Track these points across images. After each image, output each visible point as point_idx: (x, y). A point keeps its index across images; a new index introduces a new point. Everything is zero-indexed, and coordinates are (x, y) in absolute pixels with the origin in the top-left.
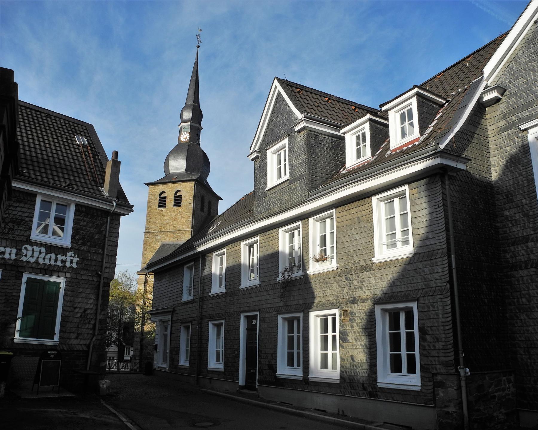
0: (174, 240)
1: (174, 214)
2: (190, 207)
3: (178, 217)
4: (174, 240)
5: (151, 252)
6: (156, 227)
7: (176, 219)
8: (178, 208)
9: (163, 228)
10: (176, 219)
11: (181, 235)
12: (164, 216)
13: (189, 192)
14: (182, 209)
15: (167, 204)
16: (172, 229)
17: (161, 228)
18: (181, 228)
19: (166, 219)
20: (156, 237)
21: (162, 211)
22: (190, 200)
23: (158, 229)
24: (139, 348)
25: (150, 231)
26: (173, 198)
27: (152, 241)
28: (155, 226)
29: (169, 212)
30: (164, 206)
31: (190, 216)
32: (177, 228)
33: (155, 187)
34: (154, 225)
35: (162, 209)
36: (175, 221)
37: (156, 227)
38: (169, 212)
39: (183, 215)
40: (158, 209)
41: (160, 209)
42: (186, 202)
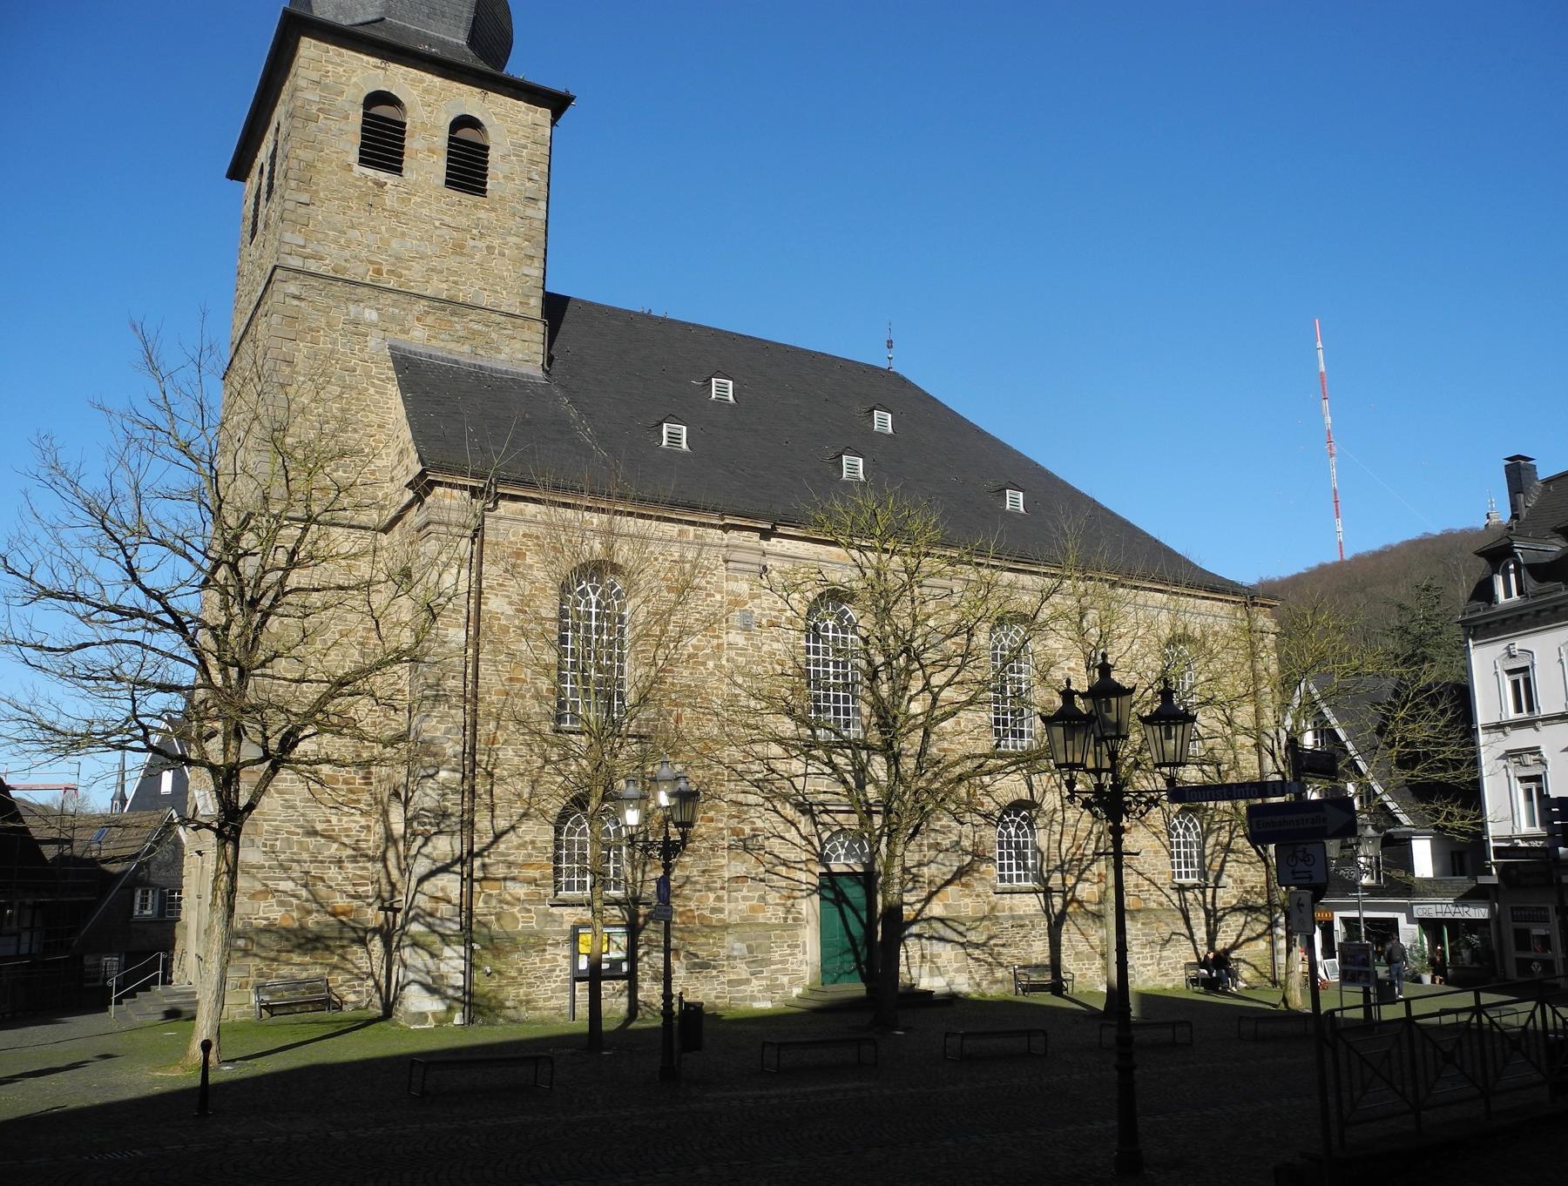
0: (452, 345)
1: (448, 220)
2: (529, 212)
3: (472, 243)
4: (452, 345)
6: (347, 253)
7: (459, 249)
8: (468, 199)
9: (389, 272)
10: (459, 249)
11: (494, 336)
12: (395, 214)
13: (525, 147)
14: (494, 210)
16: (437, 287)
17: (378, 272)
18: (485, 300)
19: (403, 234)
20: (352, 307)
21: (381, 185)
23: (358, 271)
25: (312, 266)
26: (441, 141)
27: (329, 325)
28: (342, 248)
29: (420, 205)
30: (394, 165)
31: (531, 258)
32: (464, 294)
33: (340, 55)
34: (336, 242)
35: (382, 176)
36: (458, 259)
37: (347, 253)
38: (420, 205)
39: (496, 242)
41: (370, 172)
42: (510, 185)
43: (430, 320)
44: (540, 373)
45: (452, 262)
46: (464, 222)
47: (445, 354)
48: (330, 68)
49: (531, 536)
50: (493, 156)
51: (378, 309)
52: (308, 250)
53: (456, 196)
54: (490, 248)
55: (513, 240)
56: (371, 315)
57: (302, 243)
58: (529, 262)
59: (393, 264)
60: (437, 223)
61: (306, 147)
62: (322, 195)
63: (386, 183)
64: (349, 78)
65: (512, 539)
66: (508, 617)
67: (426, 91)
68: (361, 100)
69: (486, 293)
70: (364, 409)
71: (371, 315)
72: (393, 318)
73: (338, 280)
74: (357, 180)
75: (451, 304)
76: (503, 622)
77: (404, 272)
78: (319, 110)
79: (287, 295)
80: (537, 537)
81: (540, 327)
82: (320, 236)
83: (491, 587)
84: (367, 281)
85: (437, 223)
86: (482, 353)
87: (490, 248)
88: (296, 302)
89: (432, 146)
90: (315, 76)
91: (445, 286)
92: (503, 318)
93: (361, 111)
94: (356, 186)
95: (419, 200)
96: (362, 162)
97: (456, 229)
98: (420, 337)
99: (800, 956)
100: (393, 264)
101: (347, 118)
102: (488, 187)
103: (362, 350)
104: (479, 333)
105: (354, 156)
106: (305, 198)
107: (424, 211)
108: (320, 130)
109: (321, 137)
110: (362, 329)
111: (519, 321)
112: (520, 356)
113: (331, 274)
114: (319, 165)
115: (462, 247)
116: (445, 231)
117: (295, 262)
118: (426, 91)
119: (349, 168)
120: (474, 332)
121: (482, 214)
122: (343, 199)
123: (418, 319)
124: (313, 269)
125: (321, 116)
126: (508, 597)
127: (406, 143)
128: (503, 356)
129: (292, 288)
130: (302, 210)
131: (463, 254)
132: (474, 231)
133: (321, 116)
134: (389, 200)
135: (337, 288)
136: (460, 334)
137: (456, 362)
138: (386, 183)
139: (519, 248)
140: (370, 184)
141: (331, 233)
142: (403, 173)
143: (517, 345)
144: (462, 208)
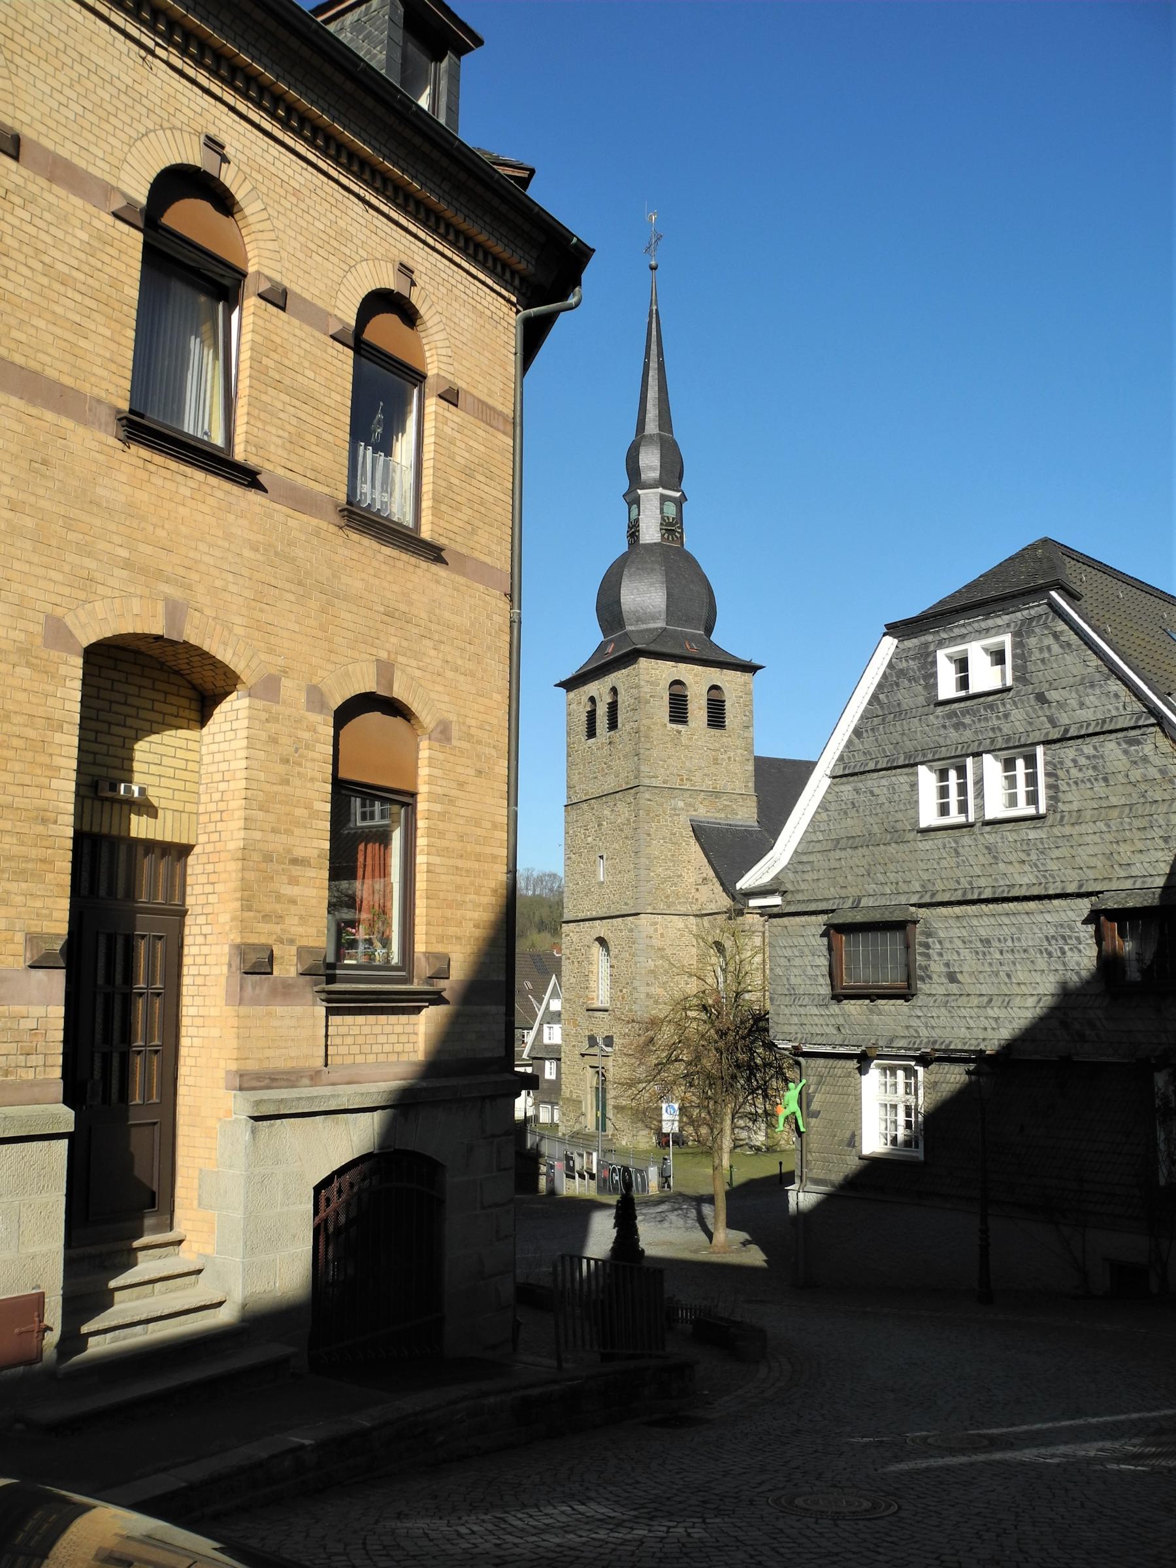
4: (717, 815)
5: (662, 841)
6: (668, 772)
7: (716, 761)
8: (717, 732)
11: (734, 806)
12: (687, 747)
14: (730, 736)
16: (708, 784)
17: (682, 780)
19: (691, 757)
21: (679, 732)
22: (744, 718)
23: (675, 782)
27: (664, 812)
28: (666, 770)
31: (748, 760)
34: (663, 767)
35: (680, 727)
39: (732, 754)
41: (674, 726)
43: (706, 803)
44: (756, 824)
45: (713, 769)
47: (713, 820)
48: (653, 672)
50: (728, 705)
53: (713, 732)
54: (729, 758)
55: (739, 751)
56: (681, 804)
67: (696, 675)
71: (681, 804)
72: (690, 805)
75: (716, 794)
81: (755, 799)
90: (647, 678)
98: (704, 812)
102: (726, 723)
104: (728, 806)
105: (667, 718)
109: (652, 710)
115: (717, 759)
117: (646, 781)
118: (696, 675)
121: (724, 739)
128: (739, 817)
129: (647, 796)
130: (647, 753)
134: (684, 741)
137: (720, 824)
139: (742, 755)
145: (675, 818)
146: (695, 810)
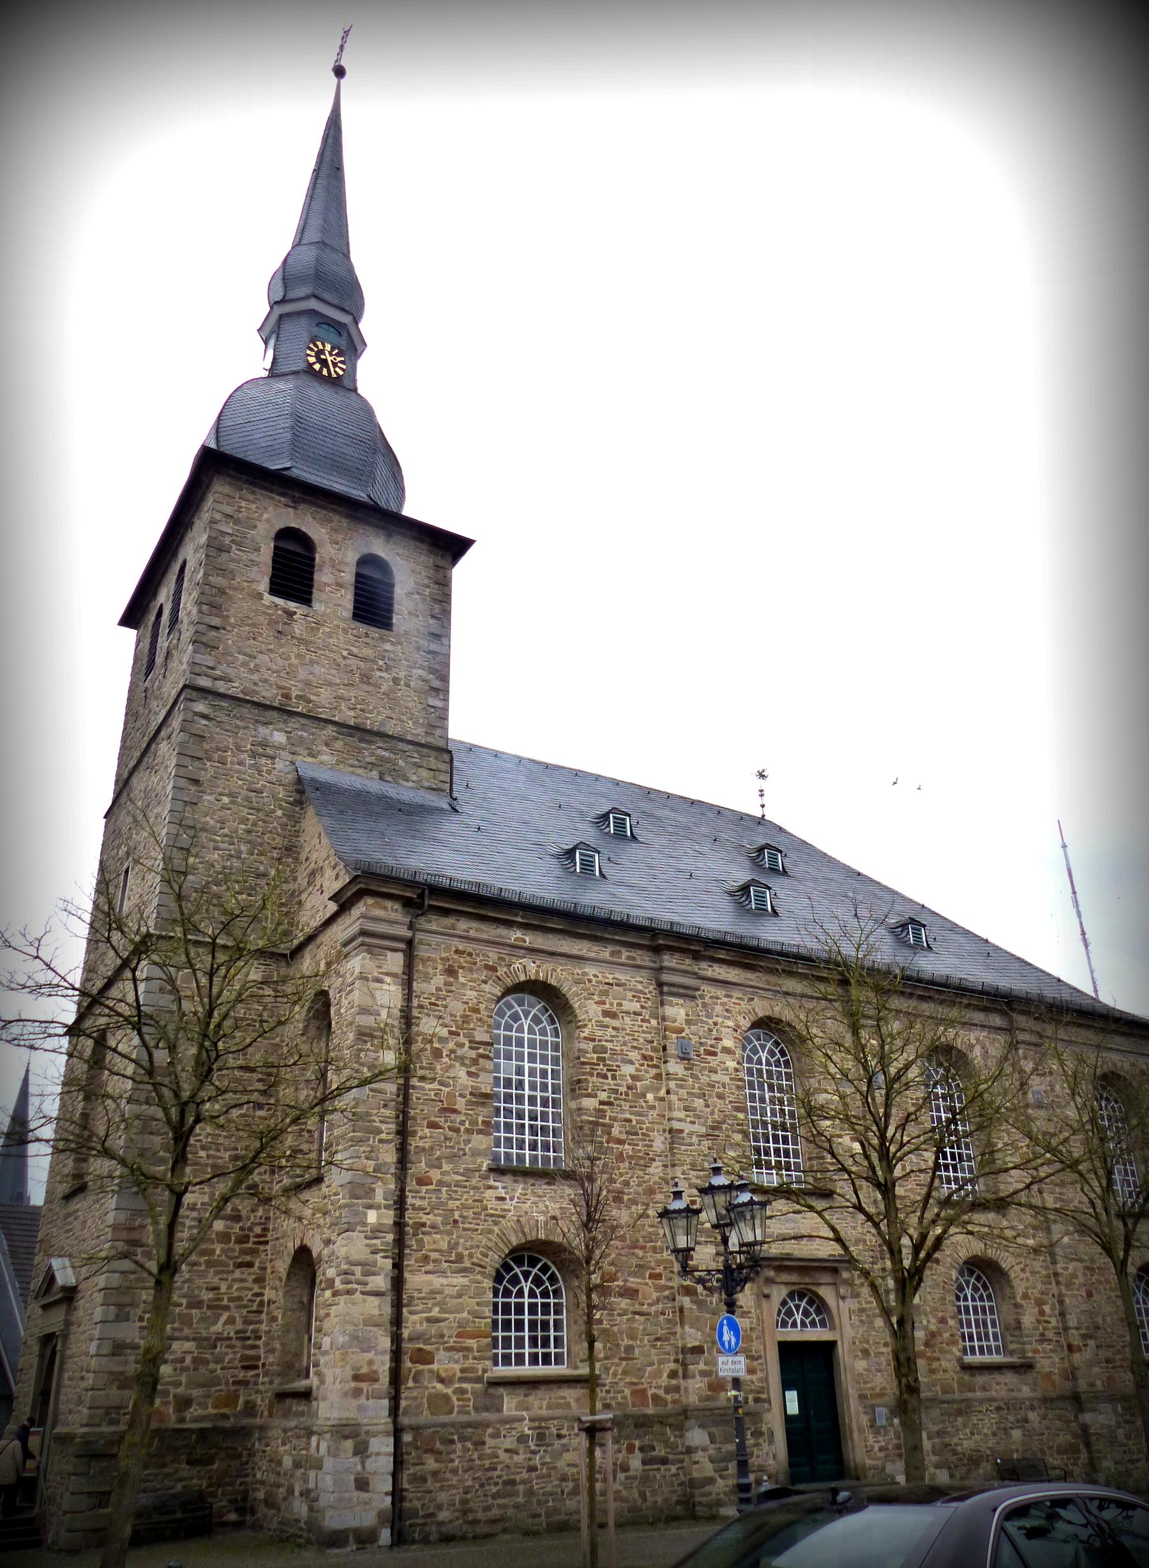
1: (355, 650)
3: (379, 674)
5: (226, 800)
6: (256, 677)
8: (375, 632)
10: (366, 678)
11: (401, 763)
14: (400, 643)
15: (316, 594)
16: (348, 716)
17: (287, 696)
18: (391, 729)
21: (290, 614)
23: (268, 694)
24: (383, 1365)
25: (221, 687)
29: (330, 635)
32: (372, 721)
34: (244, 664)
35: (292, 605)
36: (366, 688)
37: (256, 677)
38: (330, 635)
39: (402, 675)
40: (268, 598)
41: (280, 601)
43: (338, 744)
46: (368, 652)
48: (243, 504)
49: (463, 952)
51: (286, 732)
52: (218, 672)
53: (363, 628)
54: (396, 681)
56: (279, 738)
57: (211, 664)
58: (434, 694)
59: (302, 690)
60: (345, 653)
61: (218, 575)
62: (232, 620)
63: (295, 613)
64: (261, 515)
65: (444, 955)
66: (442, 1040)
68: (273, 534)
69: (393, 722)
70: (270, 832)
71: (279, 738)
73: (248, 702)
74: (268, 607)
75: (358, 732)
76: (436, 1045)
77: (312, 698)
78: (232, 541)
79: (196, 714)
80: (470, 954)
82: (230, 658)
83: (421, 1007)
84: (276, 704)
85: (345, 653)
86: (389, 779)
87: (396, 681)
88: (204, 722)
89: (340, 581)
91: (352, 713)
92: (411, 747)
93: (272, 545)
94: (266, 614)
95: (328, 630)
96: (273, 591)
97: (364, 659)
99: (765, 1447)
100: (302, 690)
101: (258, 550)
102: (394, 621)
103: (269, 772)
104: (388, 760)
105: (264, 585)
106: (216, 621)
107: (331, 641)
108: (233, 560)
109: (232, 566)
110: (269, 751)
111: (425, 751)
112: (426, 784)
113: (241, 695)
114: (231, 592)
116: (352, 661)
119: (260, 596)
120: (382, 759)
121: (388, 646)
122: (254, 625)
123: (327, 745)
124: (221, 690)
125: (234, 547)
126: (440, 1017)
127: (316, 577)
131: (369, 684)
132: (381, 663)
133: (234, 547)
134: (298, 629)
135: (245, 711)
136: (368, 760)
138: (295, 613)
140: (280, 612)
141: (241, 657)
142: (313, 604)
143: (424, 773)
144: (368, 640)
145: (263, 761)
146: (311, 755)
